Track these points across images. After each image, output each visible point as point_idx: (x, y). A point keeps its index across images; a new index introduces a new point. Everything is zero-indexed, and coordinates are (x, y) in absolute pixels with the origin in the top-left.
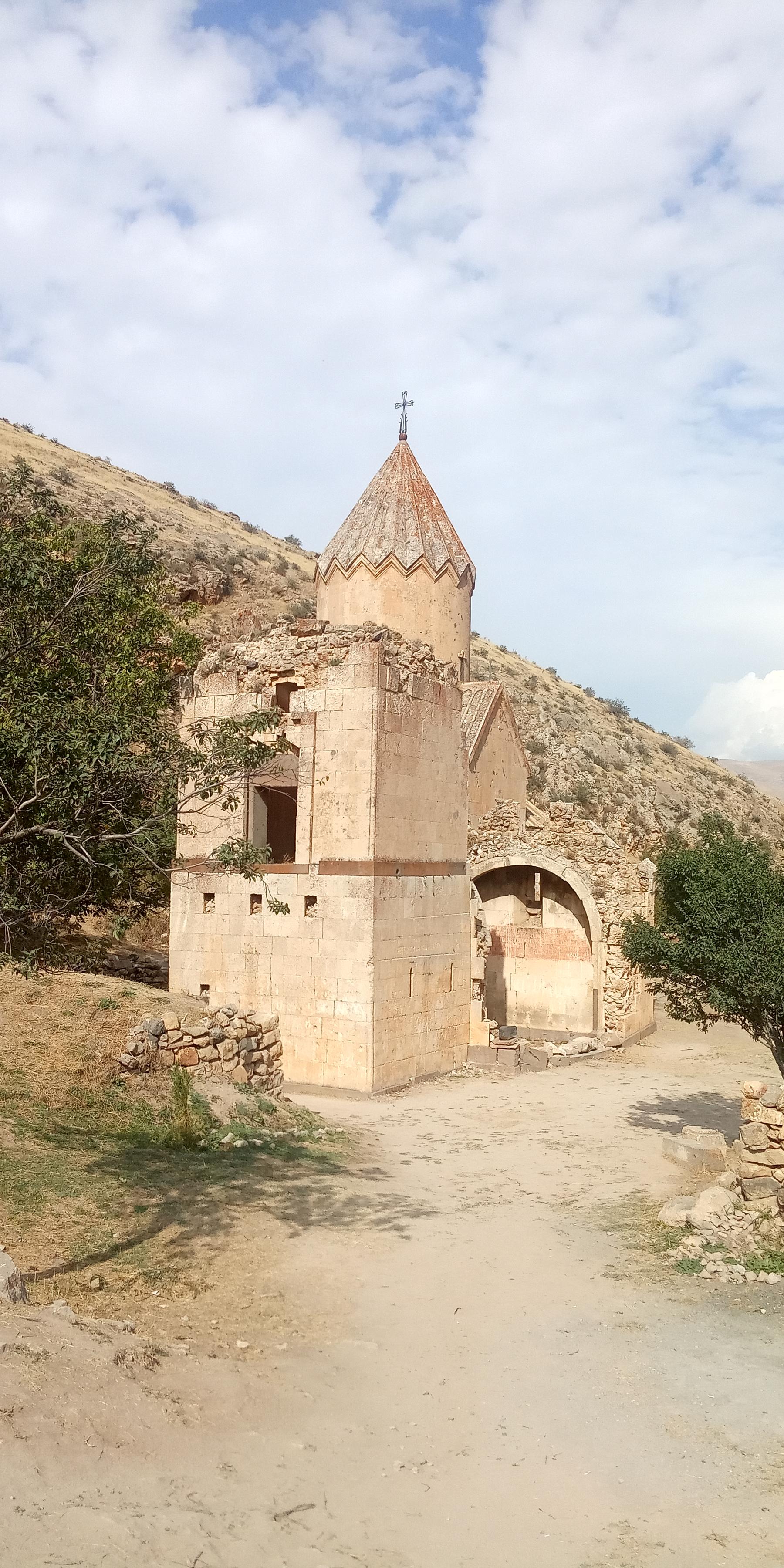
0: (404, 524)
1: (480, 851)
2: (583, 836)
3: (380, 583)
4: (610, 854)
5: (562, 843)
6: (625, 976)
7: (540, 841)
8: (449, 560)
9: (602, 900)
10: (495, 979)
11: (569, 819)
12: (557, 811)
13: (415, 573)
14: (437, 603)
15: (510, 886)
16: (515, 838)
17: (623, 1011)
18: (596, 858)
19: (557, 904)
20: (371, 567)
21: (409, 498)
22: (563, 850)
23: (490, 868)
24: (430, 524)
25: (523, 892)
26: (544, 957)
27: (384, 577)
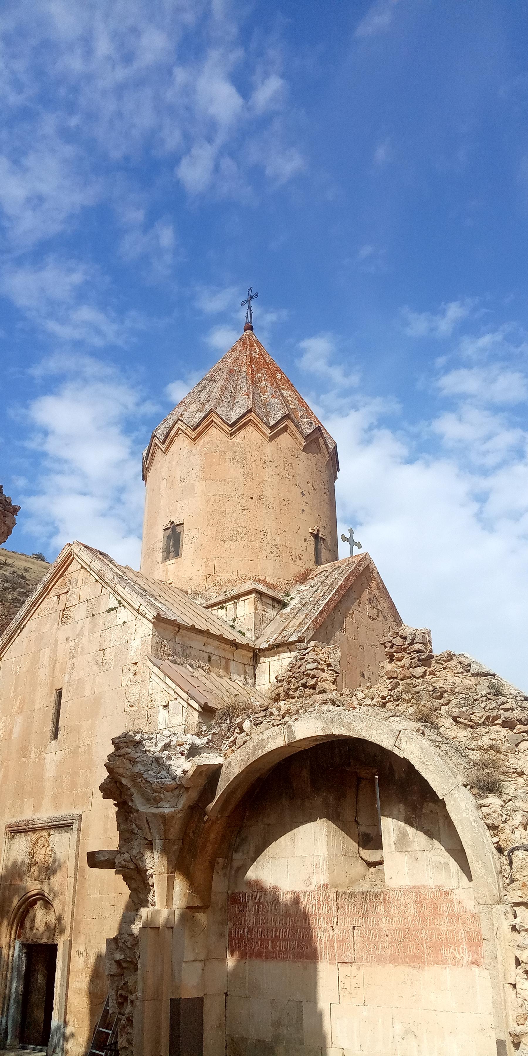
0: (235, 389)
1: (247, 725)
2: (450, 681)
3: (199, 448)
4: (507, 706)
5: (407, 696)
7: (368, 701)
8: (286, 417)
9: (493, 800)
11: (418, 651)
12: (398, 641)
13: (243, 432)
14: (273, 465)
15: (318, 801)
16: (325, 703)
18: (479, 715)
19: (411, 831)
22: (411, 710)
23: (260, 753)
24: (269, 388)
25: (349, 815)
26: (394, 960)
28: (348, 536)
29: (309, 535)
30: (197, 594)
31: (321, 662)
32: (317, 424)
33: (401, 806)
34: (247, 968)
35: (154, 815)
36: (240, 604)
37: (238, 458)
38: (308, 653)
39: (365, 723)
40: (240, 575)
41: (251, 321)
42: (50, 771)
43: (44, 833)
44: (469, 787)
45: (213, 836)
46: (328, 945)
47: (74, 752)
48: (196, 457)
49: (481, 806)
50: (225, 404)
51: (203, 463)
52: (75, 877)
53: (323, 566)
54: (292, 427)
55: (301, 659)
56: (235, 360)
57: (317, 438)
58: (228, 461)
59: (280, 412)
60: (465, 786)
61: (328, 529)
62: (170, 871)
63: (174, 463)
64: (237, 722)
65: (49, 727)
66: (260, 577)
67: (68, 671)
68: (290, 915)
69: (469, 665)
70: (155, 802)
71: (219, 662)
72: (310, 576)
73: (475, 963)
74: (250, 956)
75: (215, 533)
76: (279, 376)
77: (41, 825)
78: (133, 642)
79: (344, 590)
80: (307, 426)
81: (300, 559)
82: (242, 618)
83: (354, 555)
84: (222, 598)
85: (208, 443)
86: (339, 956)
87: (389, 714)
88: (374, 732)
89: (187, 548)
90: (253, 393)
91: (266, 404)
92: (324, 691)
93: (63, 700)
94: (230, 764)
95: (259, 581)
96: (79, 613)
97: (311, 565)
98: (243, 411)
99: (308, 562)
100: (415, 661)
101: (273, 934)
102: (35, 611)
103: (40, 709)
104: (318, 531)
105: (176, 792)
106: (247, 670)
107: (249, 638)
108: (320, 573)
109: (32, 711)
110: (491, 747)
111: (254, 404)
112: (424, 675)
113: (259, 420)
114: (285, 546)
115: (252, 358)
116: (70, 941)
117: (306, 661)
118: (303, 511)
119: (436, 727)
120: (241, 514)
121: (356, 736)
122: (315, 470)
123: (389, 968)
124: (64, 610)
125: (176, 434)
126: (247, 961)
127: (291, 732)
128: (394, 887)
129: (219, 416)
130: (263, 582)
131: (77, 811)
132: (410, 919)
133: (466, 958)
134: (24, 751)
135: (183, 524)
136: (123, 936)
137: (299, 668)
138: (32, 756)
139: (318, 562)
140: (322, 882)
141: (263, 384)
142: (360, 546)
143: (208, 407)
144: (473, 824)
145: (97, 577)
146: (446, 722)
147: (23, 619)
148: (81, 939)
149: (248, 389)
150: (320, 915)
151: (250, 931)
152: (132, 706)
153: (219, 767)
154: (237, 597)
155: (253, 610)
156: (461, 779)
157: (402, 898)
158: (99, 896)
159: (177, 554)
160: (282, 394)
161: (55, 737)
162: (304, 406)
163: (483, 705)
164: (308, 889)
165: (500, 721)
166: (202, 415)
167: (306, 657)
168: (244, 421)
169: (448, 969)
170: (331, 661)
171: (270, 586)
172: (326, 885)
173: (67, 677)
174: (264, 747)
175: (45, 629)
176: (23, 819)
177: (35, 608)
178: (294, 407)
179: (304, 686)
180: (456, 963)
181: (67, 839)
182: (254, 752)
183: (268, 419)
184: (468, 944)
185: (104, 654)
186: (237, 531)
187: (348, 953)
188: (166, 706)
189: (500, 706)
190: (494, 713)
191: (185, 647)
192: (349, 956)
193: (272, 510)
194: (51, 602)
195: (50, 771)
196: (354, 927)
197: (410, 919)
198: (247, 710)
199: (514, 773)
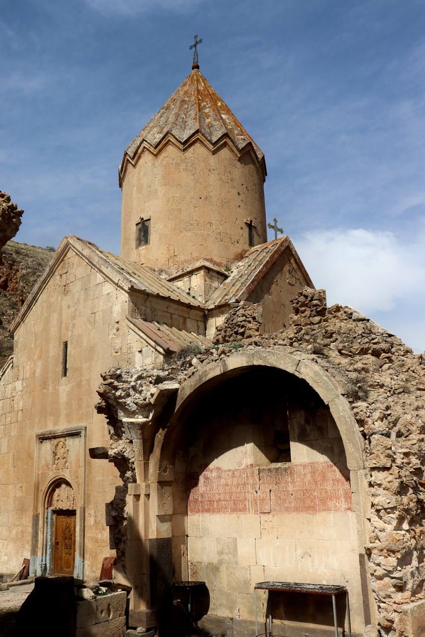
2: (338, 325)
3: (160, 161)
5: (307, 337)
6: (406, 526)
8: (226, 135)
9: (361, 405)
10: (236, 549)
11: (316, 305)
12: (302, 299)
13: (192, 148)
14: (216, 172)
16: (251, 344)
17: (407, 594)
18: (356, 346)
20: (152, 149)
21: (193, 98)
22: (310, 346)
23: (205, 379)
24: (211, 114)
26: (297, 509)
27: (163, 154)
28: (273, 224)
29: (245, 224)
30: (162, 271)
31: (248, 316)
32: (249, 140)
33: (303, 412)
34: (201, 518)
35: (132, 423)
36: (194, 276)
37: (189, 168)
38: (239, 310)
39: (276, 356)
40: (194, 256)
41: (197, 62)
42: (63, 398)
43: (62, 439)
44: (346, 396)
46: (253, 502)
47: (79, 385)
48: (158, 168)
49: (353, 408)
50: (178, 127)
51: (163, 173)
52: (85, 467)
53: (255, 247)
54: (230, 143)
55: (234, 314)
56: (186, 93)
57: (249, 151)
58: (182, 171)
59: (220, 132)
60: (343, 395)
61: (259, 220)
62: (146, 459)
63: (142, 174)
64: (188, 360)
65: (60, 368)
66: (208, 257)
67: (70, 329)
68: (228, 485)
69: (351, 314)
71: (179, 319)
72: (246, 255)
73: (349, 509)
74: (202, 512)
75: (173, 226)
76: (219, 104)
77: (59, 434)
78: (115, 307)
79: (270, 264)
80: (241, 142)
81: (238, 242)
82: (196, 288)
83: (278, 238)
84: (180, 273)
85: (166, 157)
86: (261, 509)
87: (294, 349)
88: (282, 362)
89: (153, 237)
90: (200, 117)
91: (210, 126)
92: (250, 337)
93: (68, 350)
94: (183, 388)
95: (207, 260)
96: (76, 288)
97: (246, 247)
98: (192, 131)
99: (243, 245)
100: (314, 313)
101: (217, 497)
102: (45, 287)
103: (53, 356)
104: (251, 221)
105: (147, 408)
106: (199, 325)
107: (199, 301)
108: (253, 253)
109: (48, 358)
110: (363, 369)
111: (200, 126)
112: (320, 322)
113: (204, 139)
114: (226, 233)
115: (198, 91)
116: (84, 508)
117: (238, 315)
118: (239, 206)
119: (327, 357)
120: (192, 211)
121: (269, 366)
122: (248, 175)
123: (294, 515)
124: (65, 286)
125: (143, 151)
126: (200, 515)
127: (225, 365)
128: (297, 464)
129: (174, 136)
131: (83, 424)
132: (307, 483)
133: (343, 506)
134: (44, 385)
135: (149, 220)
136: (116, 501)
137: (232, 321)
138: (50, 388)
139: (251, 244)
140: (249, 463)
141: (207, 111)
142: (282, 231)
143: (165, 130)
144: (347, 419)
145: (87, 261)
146: (334, 354)
147: (37, 293)
148: (92, 506)
149: (196, 115)
150: (248, 484)
151: (202, 496)
152: (117, 353)
153: (177, 390)
154: (191, 273)
155: (203, 281)
156: (341, 390)
157: (302, 471)
158: (101, 478)
159: (146, 242)
160: (221, 118)
161: (65, 374)
162: (238, 126)
163: (359, 341)
164: (240, 468)
165: (370, 352)
166: (161, 136)
167: (238, 313)
168: (193, 139)
169: (331, 514)
170: (255, 315)
171: (215, 263)
172: (252, 465)
173: (70, 333)
174: (206, 375)
175: (52, 300)
176: (47, 430)
177: (45, 285)
178: (231, 127)
179: (236, 333)
180: (337, 510)
181: (78, 442)
182: (200, 379)
183: (211, 137)
184: (345, 497)
185: (95, 316)
186: (190, 223)
187: (267, 507)
188: (140, 352)
189: (371, 341)
190: (367, 346)
191: (153, 310)
192: (267, 509)
193: (216, 207)
194: (56, 280)
195: (63, 398)
196: (270, 491)
197: (307, 483)
198: (196, 352)
199: (377, 385)
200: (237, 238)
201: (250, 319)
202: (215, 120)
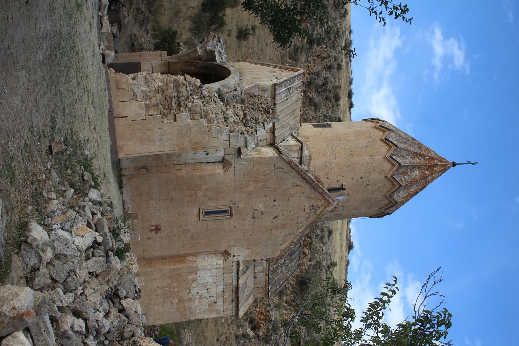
13: (384, 145)
14: (372, 160)
27: (376, 131)
40: (311, 149)
45: (193, 68)
54: (395, 169)
60: (219, 90)
70: (201, 48)
81: (327, 178)
111: (400, 148)
112: (260, 111)
118: (353, 179)
125: (377, 123)
130: (311, 160)
135: (331, 127)
139: (330, 190)
200: (330, 177)
201: (260, 101)
202: (410, 162)
